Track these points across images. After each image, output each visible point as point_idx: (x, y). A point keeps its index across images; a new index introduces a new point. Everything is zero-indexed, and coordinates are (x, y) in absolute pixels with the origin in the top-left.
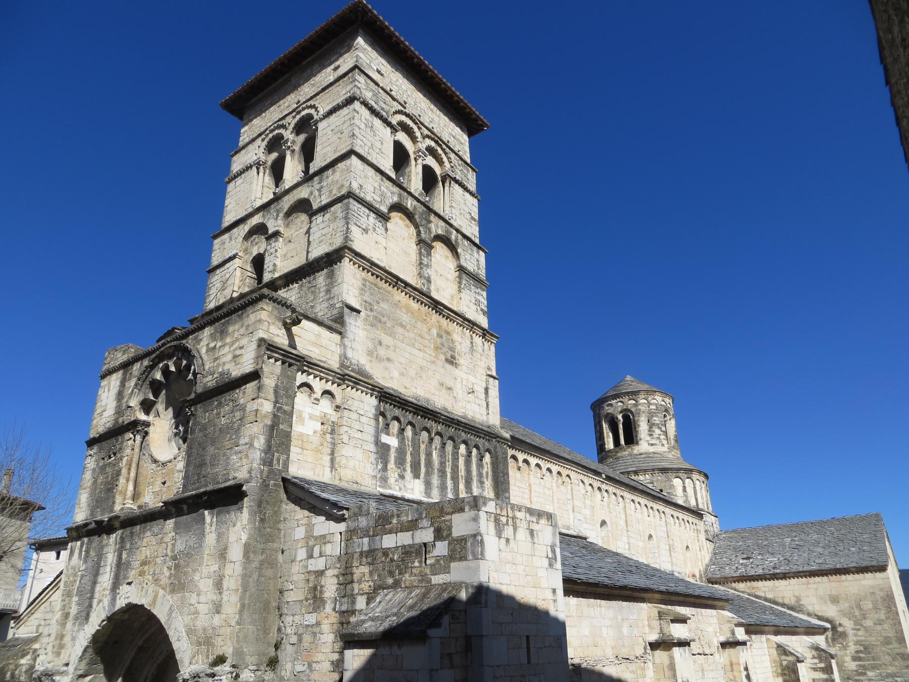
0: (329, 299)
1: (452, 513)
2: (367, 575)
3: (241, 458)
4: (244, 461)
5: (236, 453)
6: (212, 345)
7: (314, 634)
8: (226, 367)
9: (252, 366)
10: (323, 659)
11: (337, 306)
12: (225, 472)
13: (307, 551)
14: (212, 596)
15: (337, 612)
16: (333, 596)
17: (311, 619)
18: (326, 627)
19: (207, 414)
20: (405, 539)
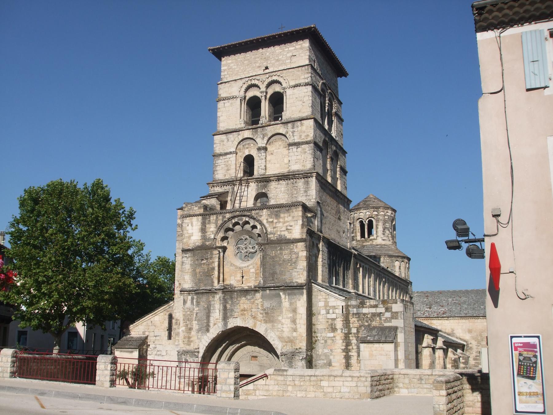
0: (307, 196)
1: (392, 304)
2: (356, 322)
3: (299, 274)
4: (301, 276)
6: (271, 220)
7: (333, 340)
8: (283, 233)
9: (300, 236)
10: (338, 348)
11: (312, 200)
13: (326, 311)
17: (332, 335)
18: (338, 338)
19: (274, 252)
20: (373, 310)
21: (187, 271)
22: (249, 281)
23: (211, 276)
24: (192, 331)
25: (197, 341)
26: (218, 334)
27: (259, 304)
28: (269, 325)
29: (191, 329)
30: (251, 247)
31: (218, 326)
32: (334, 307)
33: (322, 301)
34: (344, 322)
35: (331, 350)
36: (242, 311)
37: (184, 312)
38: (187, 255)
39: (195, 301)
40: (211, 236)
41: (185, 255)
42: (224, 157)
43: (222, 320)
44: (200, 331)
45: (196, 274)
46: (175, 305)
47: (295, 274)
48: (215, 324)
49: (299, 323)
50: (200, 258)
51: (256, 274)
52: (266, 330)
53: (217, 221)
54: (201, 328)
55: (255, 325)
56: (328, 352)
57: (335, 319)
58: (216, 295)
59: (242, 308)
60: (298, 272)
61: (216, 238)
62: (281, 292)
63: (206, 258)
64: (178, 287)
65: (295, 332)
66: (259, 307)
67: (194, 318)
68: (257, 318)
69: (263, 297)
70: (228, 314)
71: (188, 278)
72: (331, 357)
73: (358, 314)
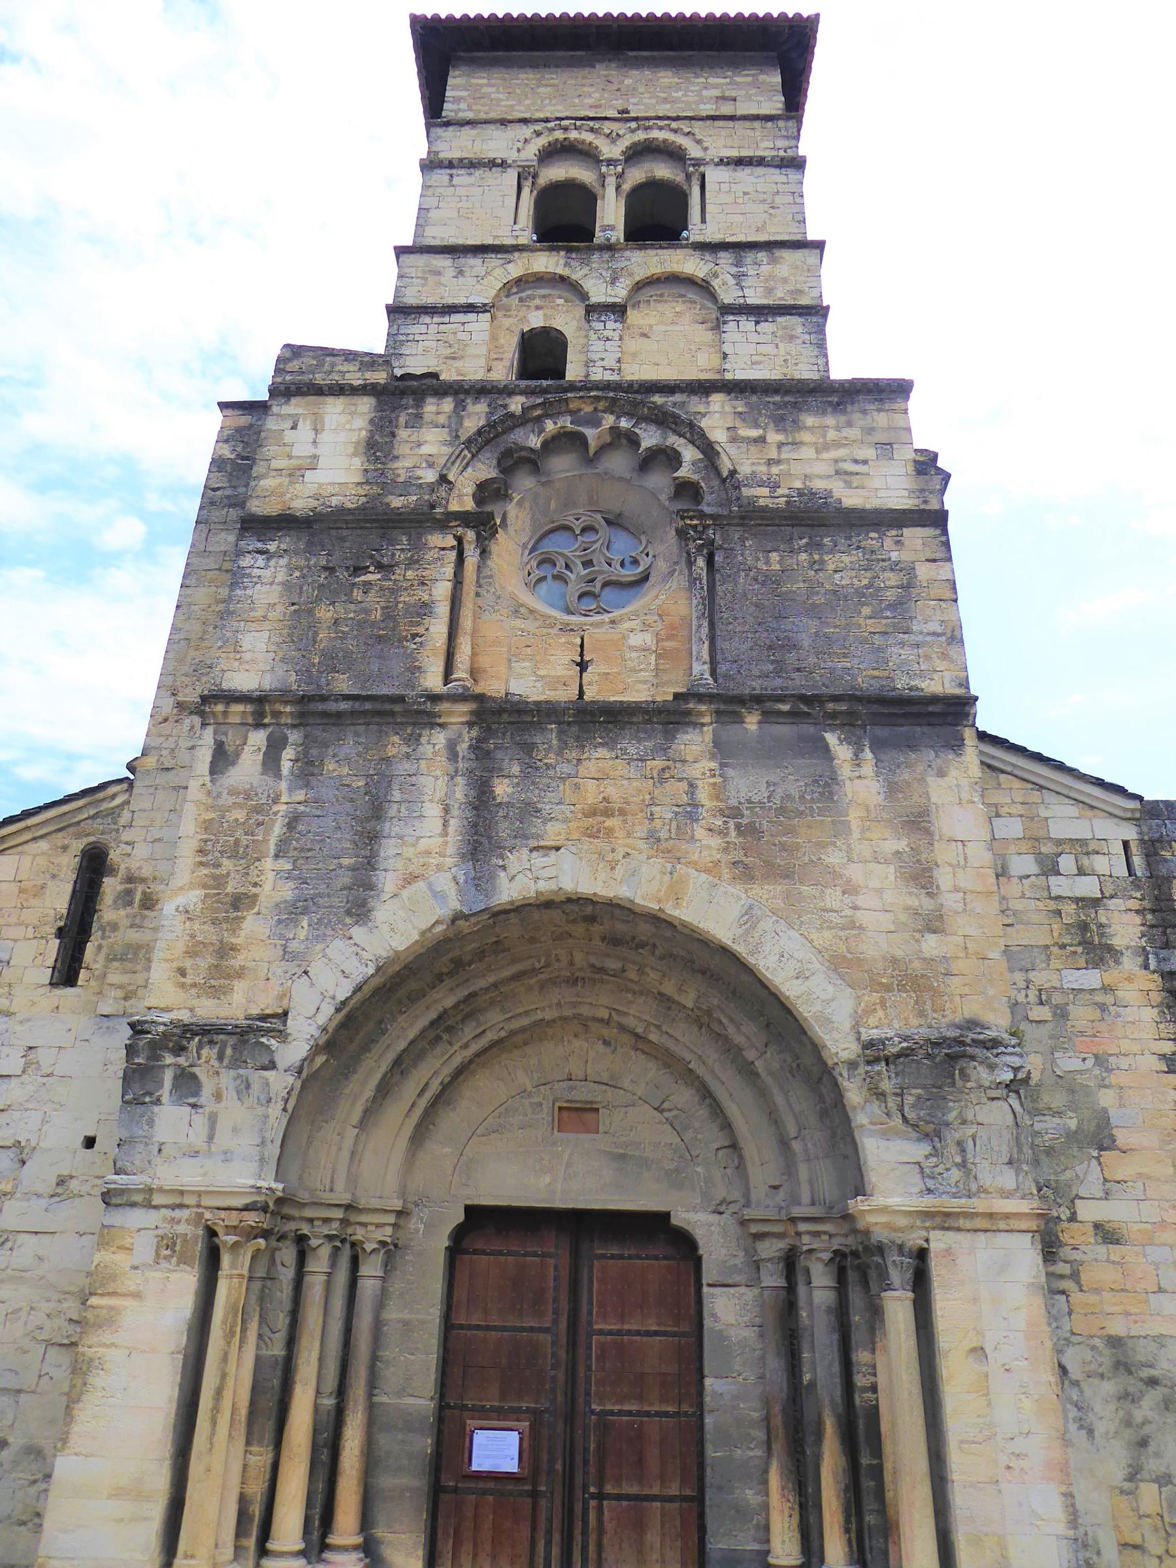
3: (928, 658)
4: (940, 665)
5: (902, 644)
7: (1103, 1007)
10: (1136, 1048)
12: (876, 673)
15: (1154, 972)
16: (1133, 944)
17: (1092, 978)
18: (1129, 993)
21: (259, 613)
22: (621, 686)
25: (278, 969)
26: (423, 934)
27: (699, 783)
28: (767, 893)
29: (239, 902)
30: (617, 558)
31: (430, 886)
32: (1082, 847)
33: (1010, 815)
34: (1149, 917)
35: (1100, 1060)
36: (592, 813)
38: (272, 547)
40: (419, 473)
41: (260, 545)
42: (437, 319)
43: (463, 856)
44: (305, 911)
45: (313, 627)
46: (132, 806)
47: (898, 654)
48: (411, 879)
50: (350, 562)
51: (659, 657)
52: (749, 916)
53: (460, 420)
55: (676, 892)
56: (1080, 1072)
57: (1098, 899)
58: (426, 732)
59: (591, 793)
60: (918, 646)
61: (451, 477)
62: (833, 731)
63: (385, 561)
64: (166, 720)
65: (935, 932)
69: (721, 750)
70: (503, 830)
72: (1106, 1099)
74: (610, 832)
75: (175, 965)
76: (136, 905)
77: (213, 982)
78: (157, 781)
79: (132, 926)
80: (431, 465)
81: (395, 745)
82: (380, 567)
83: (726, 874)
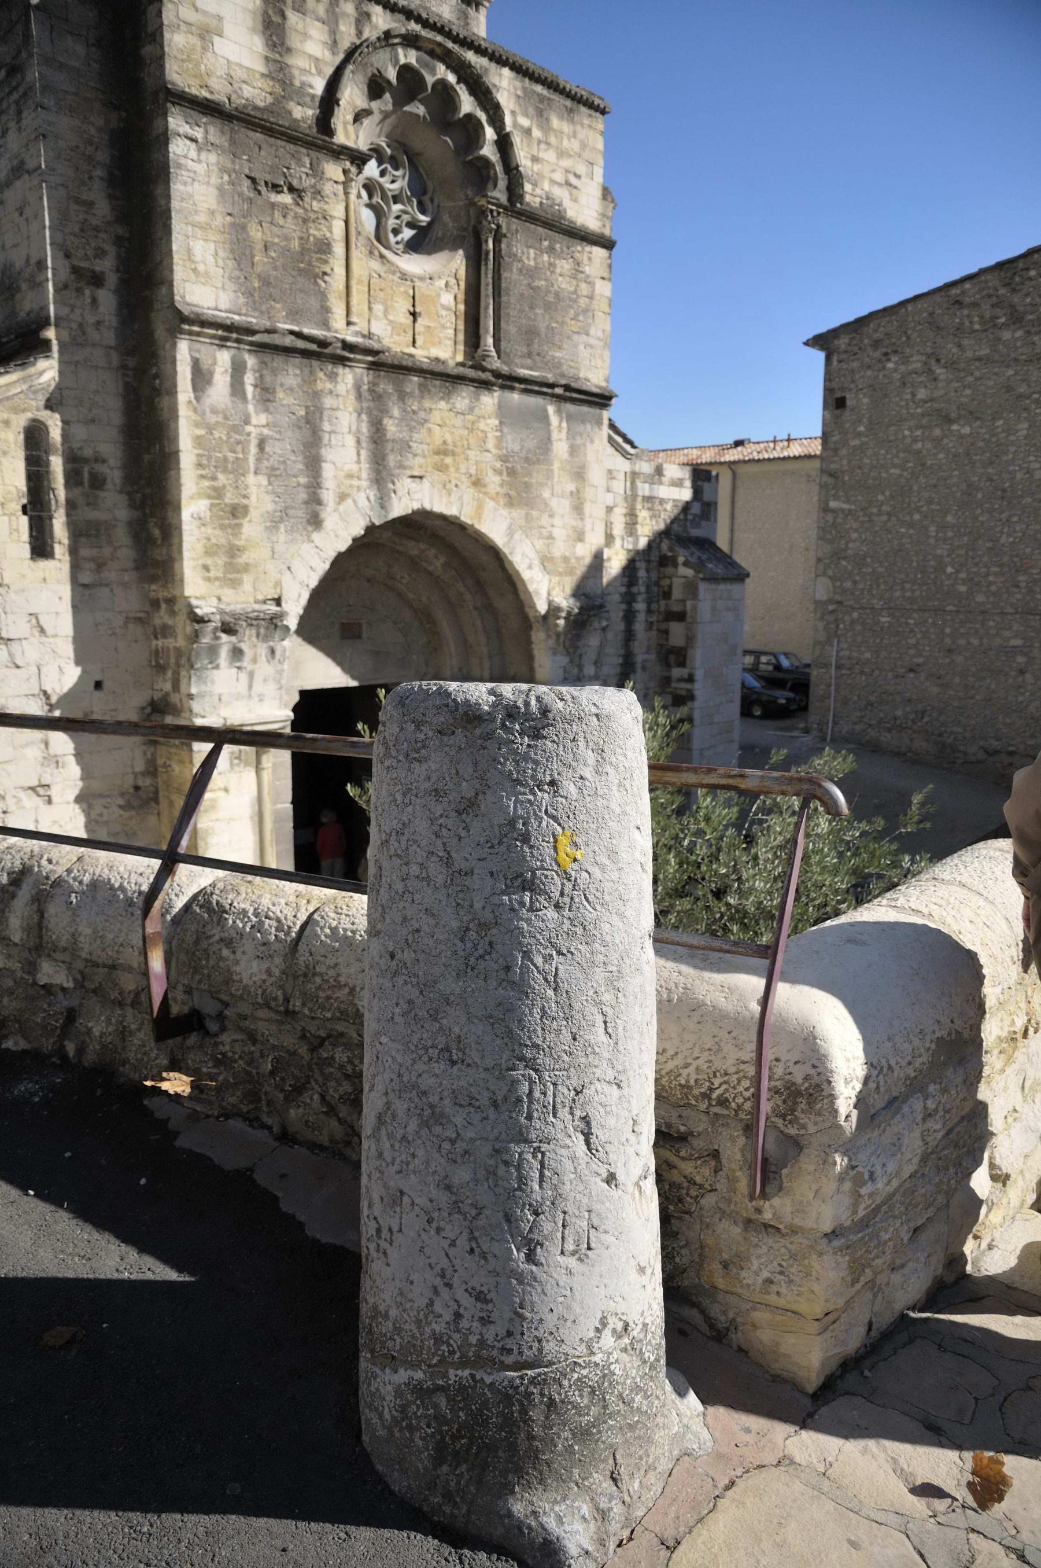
6: (525, 122)
14: (571, 521)
21: (202, 218)
23: (316, 276)
24: (245, 522)
28: (518, 513)
29: (238, 512)
37: (197, 425)
38: (198, 133)
39: (249, 379)
44: (281, 520)
47: (583, 353)
48: (342, 497)
49: (591, 517)
52: (511, 532)
54: (286, 508)
60: (591, 346)
63: (295, 183)
66: (491, 444)
67: (252, 460)
68: (485, 486)
69: (503, 412)
70: (392, 460)
71: (211, 260)
73: (649, 499)
74: (447, 467)
75: (200, 562)
76: (86, 484)
77: (229, 576)
78: (76, 358)
79: (88, 504)
80: (319, 72)
81: (323, 384)
82: (292, 189)
83: (502, 501)
